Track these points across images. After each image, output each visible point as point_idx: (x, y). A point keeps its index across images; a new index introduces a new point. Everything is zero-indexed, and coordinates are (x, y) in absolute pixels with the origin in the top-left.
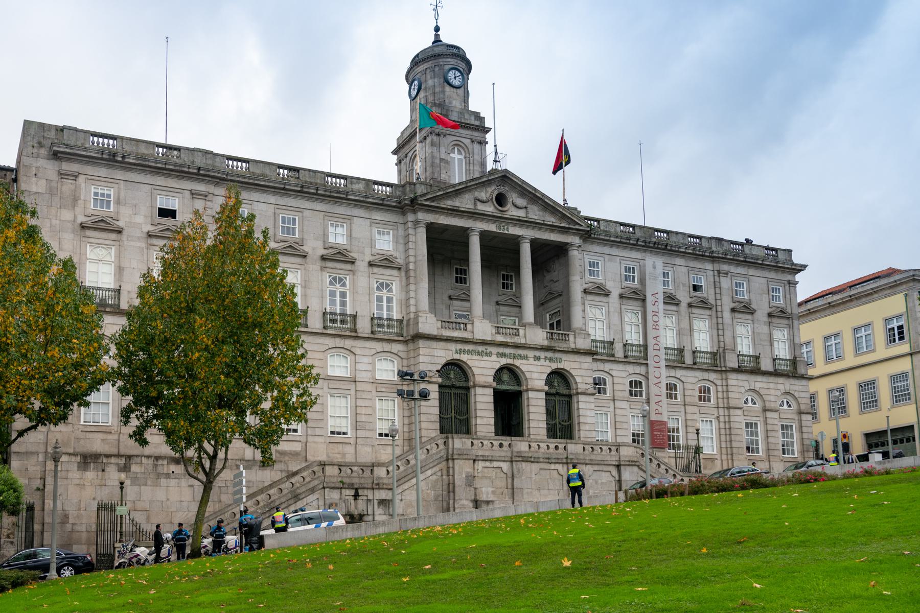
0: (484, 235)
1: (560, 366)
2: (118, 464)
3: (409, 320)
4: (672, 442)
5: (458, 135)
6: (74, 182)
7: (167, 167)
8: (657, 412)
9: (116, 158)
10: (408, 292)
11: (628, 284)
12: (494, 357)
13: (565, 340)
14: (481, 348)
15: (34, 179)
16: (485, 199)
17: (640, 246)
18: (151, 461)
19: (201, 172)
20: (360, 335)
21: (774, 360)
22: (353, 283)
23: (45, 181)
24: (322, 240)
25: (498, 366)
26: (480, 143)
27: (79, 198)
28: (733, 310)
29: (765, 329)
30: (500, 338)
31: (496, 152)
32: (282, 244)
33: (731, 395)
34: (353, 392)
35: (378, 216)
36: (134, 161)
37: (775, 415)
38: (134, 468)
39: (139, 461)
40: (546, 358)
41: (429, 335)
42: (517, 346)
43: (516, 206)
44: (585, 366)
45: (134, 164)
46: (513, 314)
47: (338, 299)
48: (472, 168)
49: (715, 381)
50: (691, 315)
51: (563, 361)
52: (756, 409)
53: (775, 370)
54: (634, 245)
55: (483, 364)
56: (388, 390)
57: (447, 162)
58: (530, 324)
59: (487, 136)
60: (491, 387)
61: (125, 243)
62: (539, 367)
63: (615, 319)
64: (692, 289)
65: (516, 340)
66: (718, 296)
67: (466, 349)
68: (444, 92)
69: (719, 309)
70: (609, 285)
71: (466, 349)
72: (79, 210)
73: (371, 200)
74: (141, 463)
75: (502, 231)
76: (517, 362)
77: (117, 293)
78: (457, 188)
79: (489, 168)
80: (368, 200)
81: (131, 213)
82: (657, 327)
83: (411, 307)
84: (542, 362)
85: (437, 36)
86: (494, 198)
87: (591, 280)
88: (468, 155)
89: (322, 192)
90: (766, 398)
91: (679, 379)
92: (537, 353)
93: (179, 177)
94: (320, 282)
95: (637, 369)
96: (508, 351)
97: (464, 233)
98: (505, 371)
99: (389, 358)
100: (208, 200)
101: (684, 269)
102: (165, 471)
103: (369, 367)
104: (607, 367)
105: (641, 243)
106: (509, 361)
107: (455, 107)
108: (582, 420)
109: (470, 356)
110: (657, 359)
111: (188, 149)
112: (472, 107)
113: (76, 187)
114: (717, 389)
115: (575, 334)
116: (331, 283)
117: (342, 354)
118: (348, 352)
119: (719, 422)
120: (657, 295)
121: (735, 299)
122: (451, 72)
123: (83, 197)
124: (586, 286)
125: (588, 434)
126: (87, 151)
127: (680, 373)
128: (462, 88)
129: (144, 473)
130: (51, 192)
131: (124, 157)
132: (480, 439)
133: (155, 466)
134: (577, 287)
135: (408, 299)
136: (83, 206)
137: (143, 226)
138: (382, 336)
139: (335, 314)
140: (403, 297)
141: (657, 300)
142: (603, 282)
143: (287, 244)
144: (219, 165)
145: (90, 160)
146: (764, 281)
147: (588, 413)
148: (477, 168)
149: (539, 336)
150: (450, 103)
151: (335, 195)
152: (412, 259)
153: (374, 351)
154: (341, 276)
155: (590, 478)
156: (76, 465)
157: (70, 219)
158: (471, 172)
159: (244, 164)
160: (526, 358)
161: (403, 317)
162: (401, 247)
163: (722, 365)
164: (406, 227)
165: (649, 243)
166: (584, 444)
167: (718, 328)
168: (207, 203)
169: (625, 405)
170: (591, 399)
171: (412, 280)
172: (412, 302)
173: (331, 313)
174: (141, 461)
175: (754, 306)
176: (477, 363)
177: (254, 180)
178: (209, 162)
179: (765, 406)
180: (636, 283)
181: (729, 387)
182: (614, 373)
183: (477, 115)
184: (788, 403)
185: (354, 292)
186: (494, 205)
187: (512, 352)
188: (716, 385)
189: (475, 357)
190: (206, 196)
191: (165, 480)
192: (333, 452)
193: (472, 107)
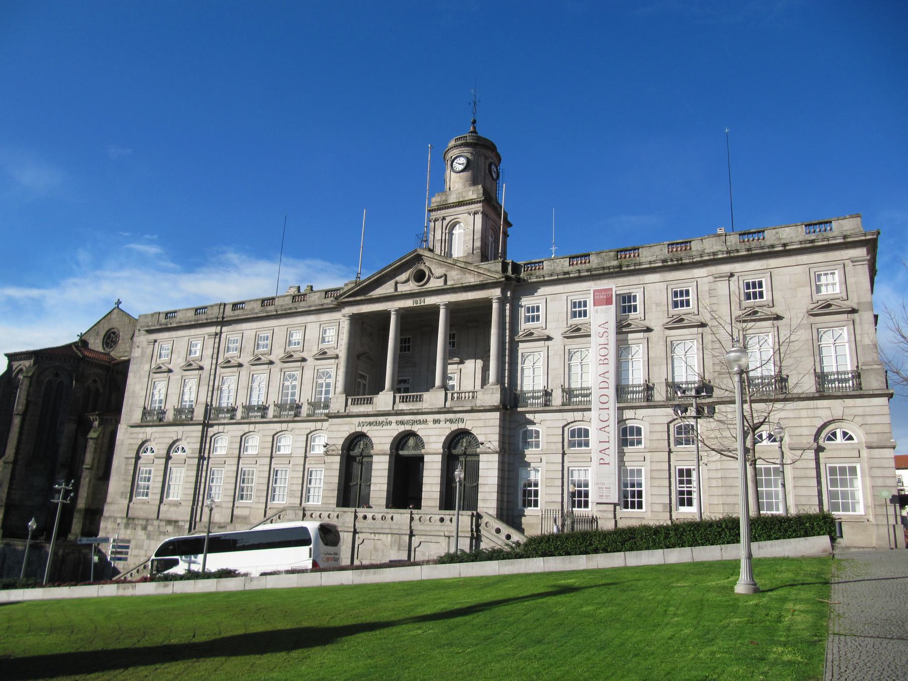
2: (142, 525)
4: (636, 499)
8: (602, 461)
12: (394, 425)
14: (381, 419)
15: (137, 349)
25: (395, 433)
38: (150, 528)
40: (446, 421)
44: (492, 423)
51: (465, 421)
55: (381, 433)
56: (316, 462)
62: (438, 430)
73: (313, 308)
74: (152, 525)
75: (418, 305)
76: (415, 428)
92: (437, 417)
102: (163, 531)
106: (408, 427)
122: (454, 163)
130: (143, 355)
133: (159, 526)
150: (454, 187)
153: (308, 431)
160: (425, 422)
165: (628, 266)
176: (376, 433)
187: (410, 419)
189: (375, 428)
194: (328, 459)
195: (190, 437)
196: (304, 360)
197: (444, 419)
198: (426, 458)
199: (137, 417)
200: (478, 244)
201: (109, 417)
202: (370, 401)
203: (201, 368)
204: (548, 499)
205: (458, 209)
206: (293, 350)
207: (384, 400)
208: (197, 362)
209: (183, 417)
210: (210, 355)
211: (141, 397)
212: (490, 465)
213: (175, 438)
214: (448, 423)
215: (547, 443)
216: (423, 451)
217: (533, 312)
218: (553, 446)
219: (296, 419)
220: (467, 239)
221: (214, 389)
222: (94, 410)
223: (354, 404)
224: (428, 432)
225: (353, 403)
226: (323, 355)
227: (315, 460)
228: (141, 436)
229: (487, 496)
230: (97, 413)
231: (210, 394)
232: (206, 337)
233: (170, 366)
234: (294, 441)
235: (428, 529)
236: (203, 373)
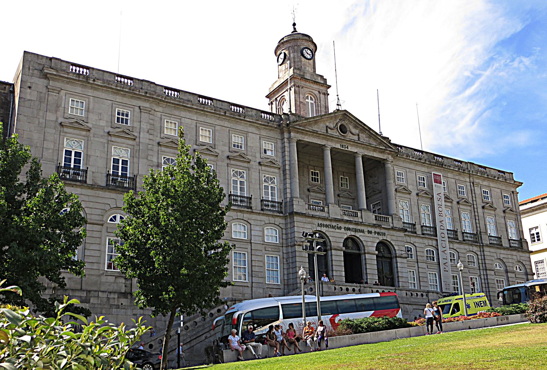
0: (333, 151)
1: (385, 238)
2: (81, 297)
3: (286, 203)
5: (310, 88)
6: (58, 95)
7: (124, 90)
9: (88, 81)
10: (285, 184)
11: (421, 187)
13: (387, 221)
14: (334, 224)
16: (333, 127)
17: (427, 164)
18: (105, 295)
19: (148, 95)
20: (254, 211)
21: (509, 240)
22: (248, 175)
23: (36, 92)
24: (228, 146)
25: (345, 237)
26: (324, 94)
27: (61, 105)
28: (483, 207)
29: (503, 221)
30: (346, 218)
31: (338, 99)
32: (201, 147)
33: (487, 262)
35: (264, 133)
36: (101, 84)
37: (513, 275)
39: (97, 295)
42: (357, 223)
43: (352, 133)
45: (101, 86)
46: (349, 204)
47: (239, 186)
48: (319, 109)
49: (476, 252)
50: (460, 209)
52: (502, 271)
53: (511, 247)
54: (424, 163)
55: (335, 234)
56: (273, 250)
57: (304, 104)
58: (364, 209)
59: (329, 90)
60: (342, 251)
61: (92, 138)
64: (458, 193)
65: (356, 219)
66: (474, 199)
68: (301, 61)
69: (475, 206)
70: (410, 188)
72: (60, 113)
74: (98, 297)
75: (344, 149)
76: (358, 235)
77: (85, 173)
78: (316, 119)
79: (331, 111)
80: (258, 122)
81: (97, 118)
82: (442, 215)
83: (288, 194)
85: (295, 29)
86: (338, 127)
87: (399, 184)
88: (317, 101)
89: (229, 115)
90: (507, 264)
91: (456, 250)
92: (370, 229)
93: (132, 97)
94: (227, 174)
95: (430, 242)
96: (351, 226)
97: (322, 148)
98: (350, 240)
99: (273, 228)
100: (151, 114)
101: (454, 181)
102: (116, 304)
103: (261, 234)
104: (413, 240)
105: (428, 163)
106: (353, 233)
107: (308, 71)
108: (400, 275)
111: (138, 80)
112: (318, 72)
113: (58, 98)
114: (478, 257)
115: (392, 218)
116: (234, 175)
117: (241, 224)
118: (246, 222)
119: (481, 279)
121: (484, 201)
123: (63, 106)
124: (396, 187)
125: (404, 284)
126: (68, 75)
127: (456, 246)
128: (312, 60)
129: (100, 304)
131: (94, 80)
132: (340, 285)
133: (108, 299)
134: (392, 188)
135: (285, 189)
136: (63, 111)
137: (105, 128)
138: (269, 213)
139: (237, 196)
140: (282, 187)
142: (406, 185)
143: (204, 147)
144: (159, 92)
145: (70, 81)
146: (499, 191)
147: (404, 270)
148: (323, 109)
149: (370, 218)
150: (305, 68)
151: (237, 117)
152: (287, 162)
153: (263, 223)
155: (411, 314)
157: (54, 119)
158: (319, 111)
159: (176, 93)
160: (363, 231)
161: (282, 201)
162: (280, 155)
163: (480, 242)
164: (283, 142)
166: (406, 291)
167: (475, 218)
168: (151, 116)
169: (424, 266)
170: (405, 261)
171: (288, 176)
172: (288, 191)
173: (234, 195)
174: (98, 295)
175: (495, 206)
176: (332, 234)
177: (183, 103)
178: (153, 89)
179: (507, 269)
180: (426, 187)
181: (485, 256)
183: (322, 77)
184: (519, 268)
185: (249, 182)
186: (338, 131)
188: (478, 255)
189: (331, 230)
190: (150, 111)
191: (116, 309)
192: (236, 292)
193: (318, 72)
205: (312, 85)
214: (376, 234)
227: (271, 248)
232: (137, 109)
235: (416, 301)
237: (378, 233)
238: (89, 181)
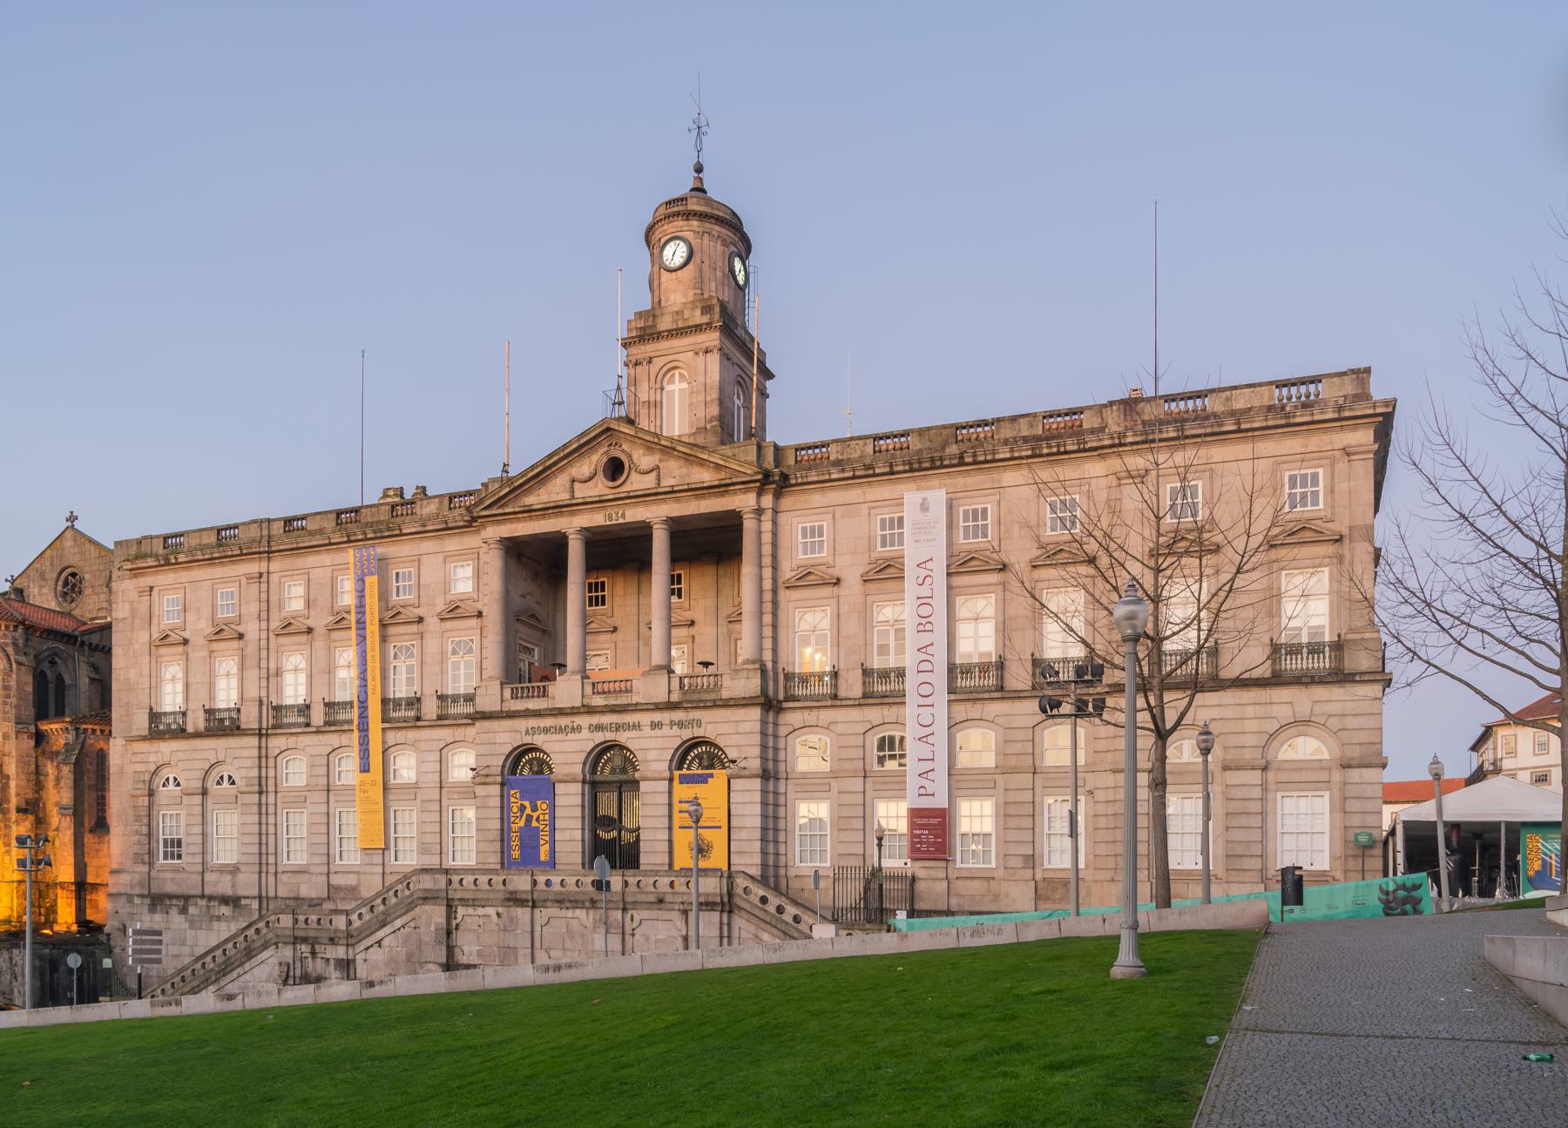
1: (698, 732)
12: (585, 732)
14: (563, 721)
25: (591, 745)
30: (598, 701)
34: (418, 801)
40: (672, 724)
41: (490, 712)
44: (747, 727)
51: (703, 725)
55: (567, 746)
63: (851, 627)
67: (542, 726)
71: (542, 726)
76: (623, 737)
84: (666, 730)
92: (657, 716)
96: (607, 719)
105: (901, 468)
106: (609, 736)
109: (548, 737)
110: (926, 690)
120: (929, 565)
141: (929, 573)
153: (442, 744)
154: (407, 643)
156: (147, 907)
160: (636, 726)
176: (557, 747)
182: (839, 728)
186: (627, 477)
194: (480, 790)
195: (238, 755)
196: (421, 620)
197: (668, 722)
198: (644, 786)
199: (141, 723)
200: (714, 411)
201: (90, 726)
202: (544, 693)
203: (241, 636)
204: (842, 849)
206: (402, 603)
207: (566, 690)
208: (233, 627)
209: (221, 726)
210: (256, 614)
211: (143, 689)
212: (747, 797)
213: (213, 762)
214: (675, 727)
215: (839, 759)
216: (637, 775)
217: (813, 536)
218: (849, 766)
219: (419, 724)
220: (694, 400)
221: (273, 676)
222: (60, 713)
223: (517, 698)
224: (645, 744)
225: (514, 697)
226: (453, 612)
228: (152, 758)
229: (745, 846)
230: (67, 719)
231: (264, 683)
233: (187, 635)
234: (420, 762)
236: (246, 646)
237: (680, 724)
238: (190, 729)
